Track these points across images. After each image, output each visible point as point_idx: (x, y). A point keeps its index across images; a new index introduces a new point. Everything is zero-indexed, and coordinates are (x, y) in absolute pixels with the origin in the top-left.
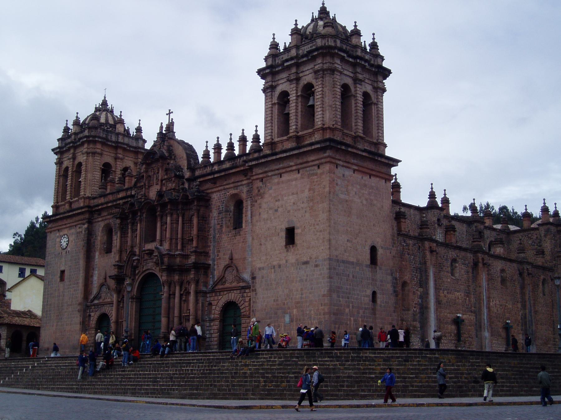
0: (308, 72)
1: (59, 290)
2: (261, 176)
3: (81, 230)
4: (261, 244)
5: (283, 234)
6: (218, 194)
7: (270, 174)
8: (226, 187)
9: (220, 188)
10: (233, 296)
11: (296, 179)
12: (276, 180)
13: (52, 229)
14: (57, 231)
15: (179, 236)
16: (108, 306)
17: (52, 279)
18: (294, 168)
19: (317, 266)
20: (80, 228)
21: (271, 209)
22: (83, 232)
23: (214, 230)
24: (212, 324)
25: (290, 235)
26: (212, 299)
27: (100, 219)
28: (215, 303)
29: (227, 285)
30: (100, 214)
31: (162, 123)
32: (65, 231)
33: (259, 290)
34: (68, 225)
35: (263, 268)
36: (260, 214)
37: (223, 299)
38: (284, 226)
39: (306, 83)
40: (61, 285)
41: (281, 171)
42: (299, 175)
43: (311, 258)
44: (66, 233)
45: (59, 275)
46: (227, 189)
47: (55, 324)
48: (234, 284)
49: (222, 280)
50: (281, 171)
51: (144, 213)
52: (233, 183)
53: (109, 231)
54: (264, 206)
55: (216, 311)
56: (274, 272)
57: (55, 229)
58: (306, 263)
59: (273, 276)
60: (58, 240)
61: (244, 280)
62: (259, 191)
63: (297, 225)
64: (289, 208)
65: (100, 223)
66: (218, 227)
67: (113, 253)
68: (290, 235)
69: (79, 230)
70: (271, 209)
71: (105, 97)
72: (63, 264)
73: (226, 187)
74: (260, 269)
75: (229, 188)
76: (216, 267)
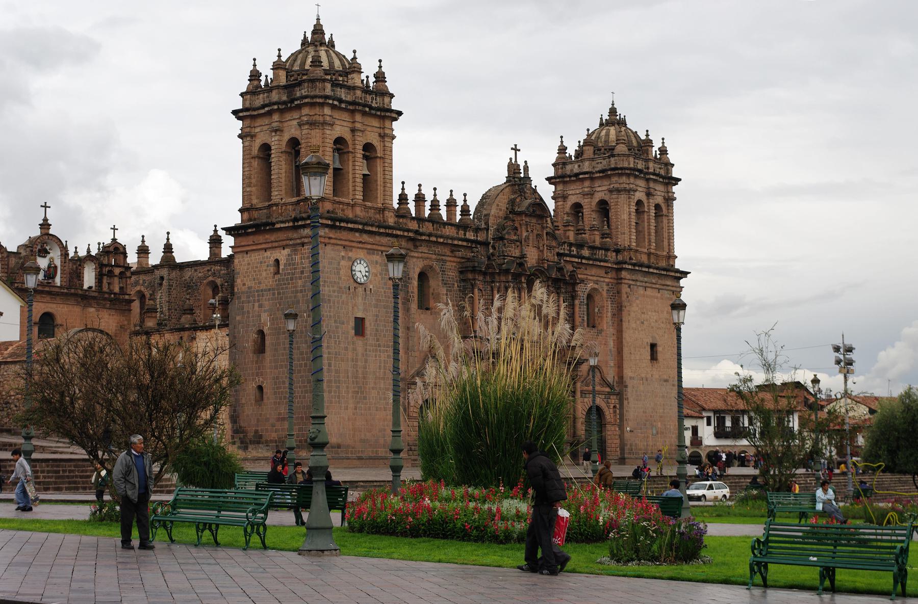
0: (659, 193)
1: (354, 349)
7: (638, 284)
11: (657, 298)
12: (641, 291)
13: (332, 241)
14: (341, 248)
17: (337, 327)
18: (657, 286)
21: (639, 319)
27: (416, 255)
30: (416, 247)
33: (631, 399)
34: (369, 246)
38: (650, 341)
40: (359, 342)
41: (647, 285)
42: (659, 295)
44: (362, 256)
45: (352, 324)
47: (351, 406)
50: (647, 285)
53: (423, 276)
54: (632, 314)
57: (339, 242)
58: (666, 381)
59: (642, 388)
60: (343, 263)
61: (609, 385)
63: (659, 343)
64: (653, 324)
65: (415, 260)
70: (639, 319)
71: (318, 19)
72: (361, 307)
74: (631, 378)
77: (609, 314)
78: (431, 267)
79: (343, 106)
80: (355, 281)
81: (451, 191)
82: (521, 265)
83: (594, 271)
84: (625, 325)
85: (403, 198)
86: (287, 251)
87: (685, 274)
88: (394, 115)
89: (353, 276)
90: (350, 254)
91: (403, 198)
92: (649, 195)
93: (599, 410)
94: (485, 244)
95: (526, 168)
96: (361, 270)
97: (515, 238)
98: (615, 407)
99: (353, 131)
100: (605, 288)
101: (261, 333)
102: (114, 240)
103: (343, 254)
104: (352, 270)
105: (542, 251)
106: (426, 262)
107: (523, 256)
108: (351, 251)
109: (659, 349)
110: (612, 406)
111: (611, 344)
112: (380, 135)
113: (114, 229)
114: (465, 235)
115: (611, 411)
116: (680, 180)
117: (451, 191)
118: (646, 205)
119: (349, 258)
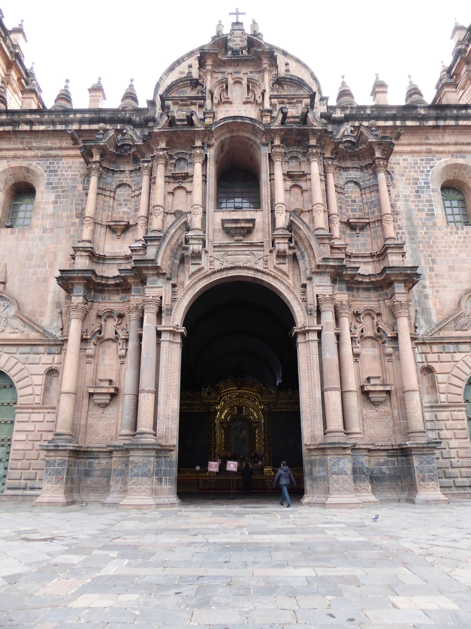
6: (410, 158)
8: (434, 148)
9: (417, 148)
15: (334, 209)
16: (13, 349)
23: (409, 219)
24: (443, 415)
26: (431, 357)
28: (447, 367)
46: (437, 152)
49: (454, 319)
51: (209, 146)
52: (456, 144)
66: (423, 215)
67: (37, 232)
73: (434, 148)
75: (442, 152)
76: (428, 291)
78: (28, 170)
81: (100, 79)
83: (449, 138)
97: (193, 94)
106: (14, 164)
117: (100, 79)
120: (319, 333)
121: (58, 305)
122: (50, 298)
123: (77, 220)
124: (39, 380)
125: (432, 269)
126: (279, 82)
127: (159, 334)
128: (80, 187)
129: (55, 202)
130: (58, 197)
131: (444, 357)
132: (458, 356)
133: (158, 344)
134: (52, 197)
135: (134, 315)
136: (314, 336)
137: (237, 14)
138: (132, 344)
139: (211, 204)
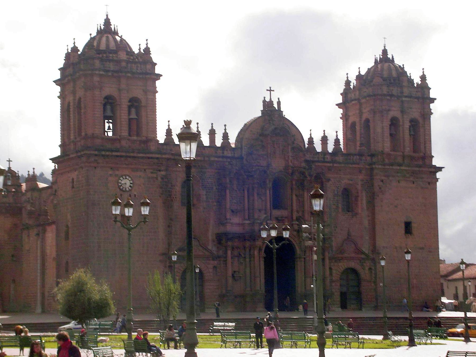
2: (383, 178)
3: (155, 175)
4: (383, 229)
5: (403, 226)
10: (352, 264)
19: (430, 252)
20: (152, 173)
22: (159, 179)
25: (408, 227)
29: (346, 255)
31: (264, 98)
32: (127, 172)
35: (387, 247)
36: (382, 206)
37: (343, 265)
38: (404, 219)
39: (413, 117)
43: (425, 246)
48: (353, 255)
55: (336, 274)
56: (397, 251)
58: (422, 248)
61: (363, 253)
62: (380, 188)
66: (334, 207)
68: (408, 227)
69: (150, 175)
71: (107, 15)
74: (384, 247)
77: (364, 202)
79: (110, 74)
80: (121, 190)
82: (265, 172)
84: (377, 209)
85: (169, 132)
86: (76, 173)
87: (440, 169)
88: (155, 77)
89: (119, 187)
90: (117, 173)
91: (169, 132)
92: (402, 112)
93: (354, 271)
94: (241, 158)
95: (279, 103)
96: (126, 183)
98: (370, 269)
99: (120, 90)
100: (360, 183)
101: (67, 226)
102: (9, 168)
103: (111, 172)
104: (118, 183)
105: (288, 161)
107: (268, 166)
108: (118, 170)
109: (414, 225)
110: (367, 268)
111: (366, 222)
112: (143, 91)
113: (9, 161)
114: (223, 153)
115: (367, 272)
116: (435, 99)
118: (401, 120)
119: (116, 175)
120: (305, 258)
121: (214, 241)
122: (210, 238)
123: (215, 204)
124: (211, 270)
125: (335, 230)
126: (293, 148)
127: (260, 257)
128: (215, 188)
129: (206, 195)
130: (207, 192)
131: (336, 264)
132: (340, 264)
133: (260, 261)
134: (204, 193)
135: (248, 250)
136: (303, 260)
137: (270, 90)
138: (248, 260)
139: (272, 207)
